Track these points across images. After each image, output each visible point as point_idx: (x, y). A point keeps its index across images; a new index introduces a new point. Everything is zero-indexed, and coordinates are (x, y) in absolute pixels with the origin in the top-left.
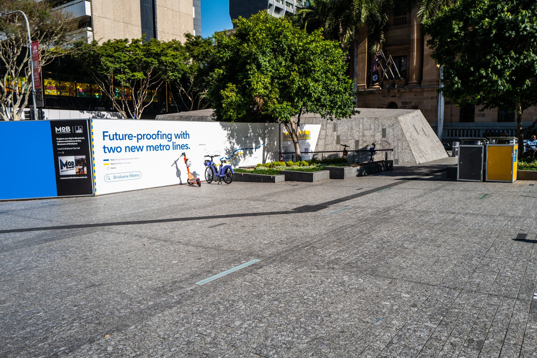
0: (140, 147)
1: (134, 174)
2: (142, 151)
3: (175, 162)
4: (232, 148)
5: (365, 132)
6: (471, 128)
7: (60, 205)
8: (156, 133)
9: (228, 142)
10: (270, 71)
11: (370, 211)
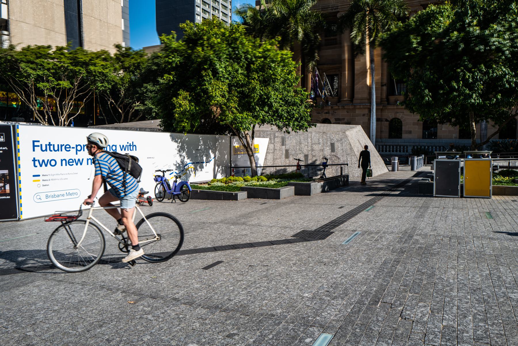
0: (79, 160)
1: (71, 192)
2: (81, 164)
4: (182, 162)
5: (314, 146)
6: (400, 144)
9: (178, 155)
10: (227, 78)
11: (390, 237)
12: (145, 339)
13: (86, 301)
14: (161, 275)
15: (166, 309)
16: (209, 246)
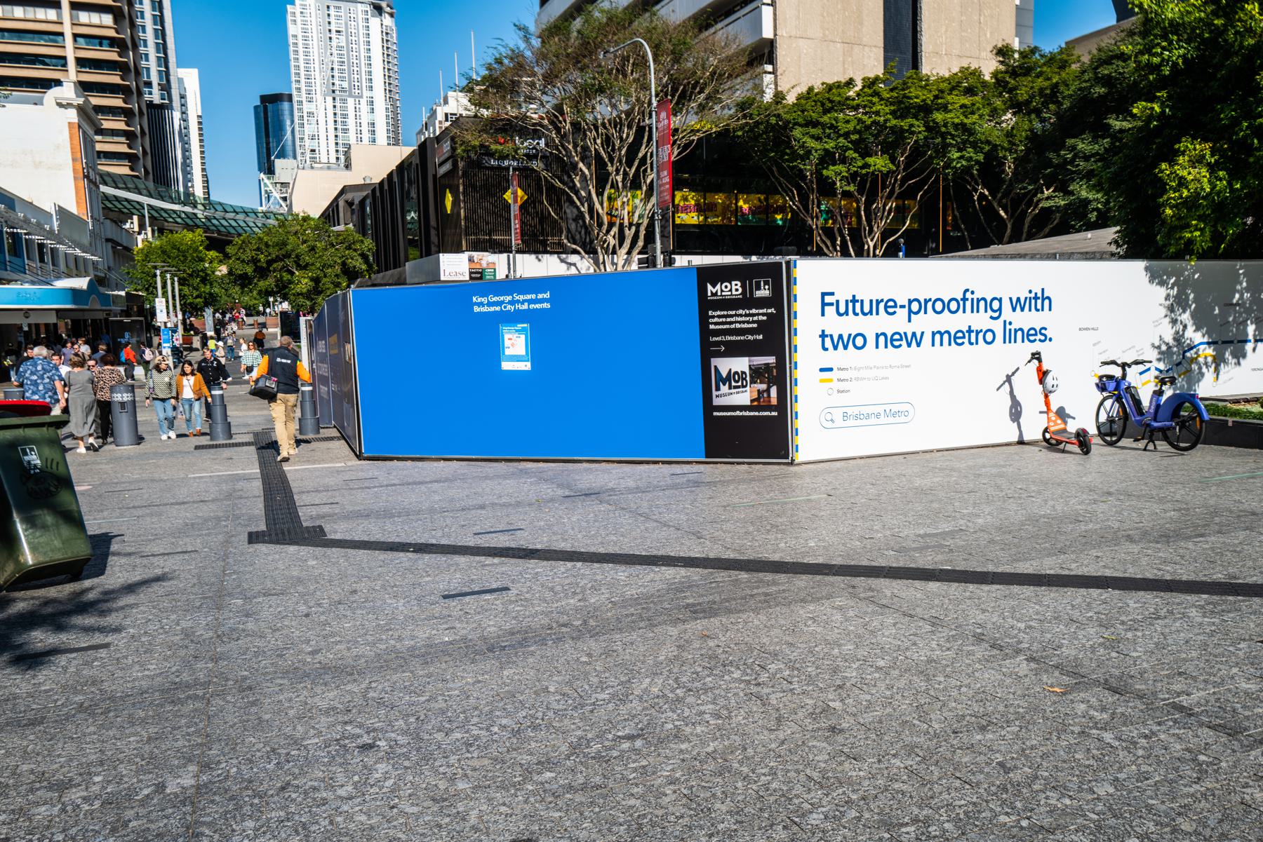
0: (914, 334)
1: (895, 408)
2: (918, 345)
3: (1009, 379)
4: (1178, 338)
8: (959, 297)
9: (1168, 319)
12: (1101, 792)
13: (944, 662)
14: (1130, 635)
15: (1155, 728)
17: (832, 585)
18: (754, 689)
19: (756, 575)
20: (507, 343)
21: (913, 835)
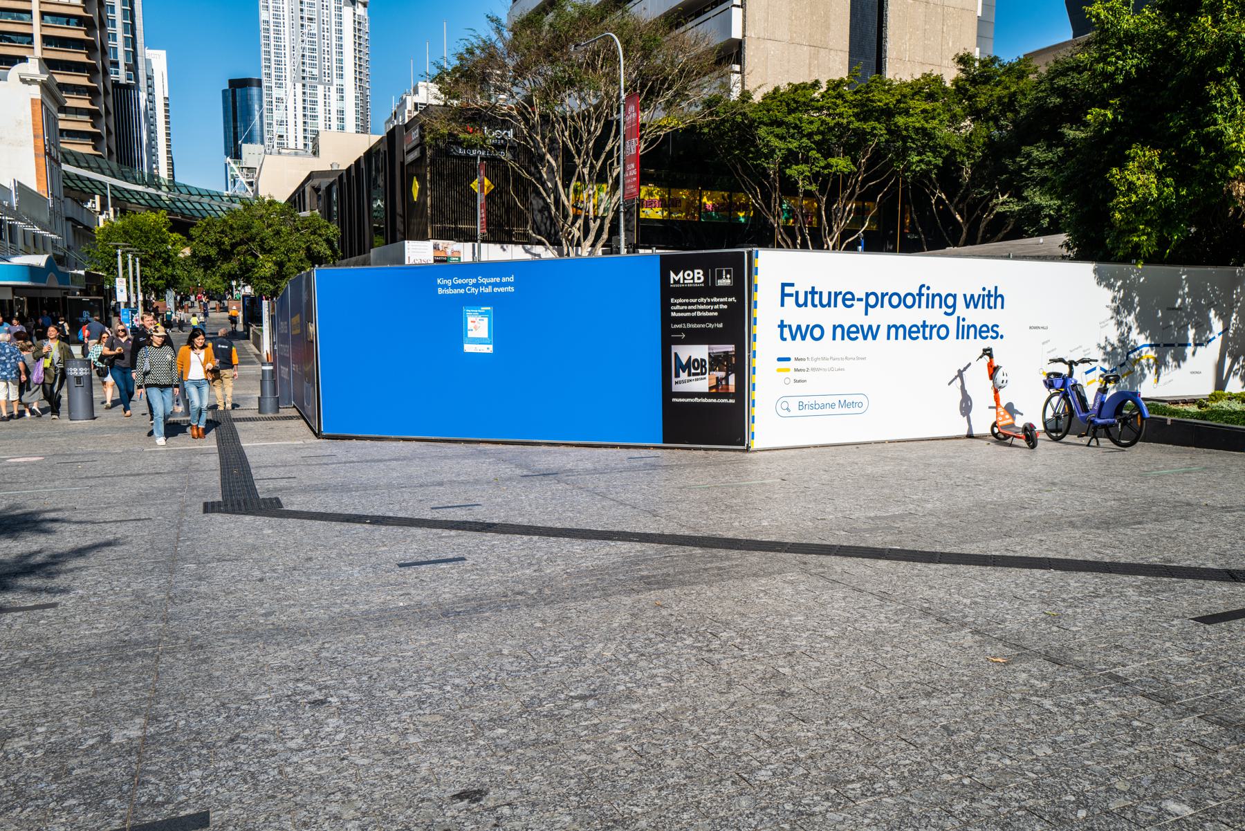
0: (870, 327)
1: (849, 399)
2: (874, 338)
3: (960, 374)
4: (1123, 341)
7: (671, 467)
8: (915, 292)
9: (1114, 321)
12: (1040, 753)
14: (1070, 611)
15: (1092, 696)
16: (1210, 565)
17: (785, 561)
18: (706, 655)
19: (709, 550)
20: (470, 325)
21: (859, 791)
